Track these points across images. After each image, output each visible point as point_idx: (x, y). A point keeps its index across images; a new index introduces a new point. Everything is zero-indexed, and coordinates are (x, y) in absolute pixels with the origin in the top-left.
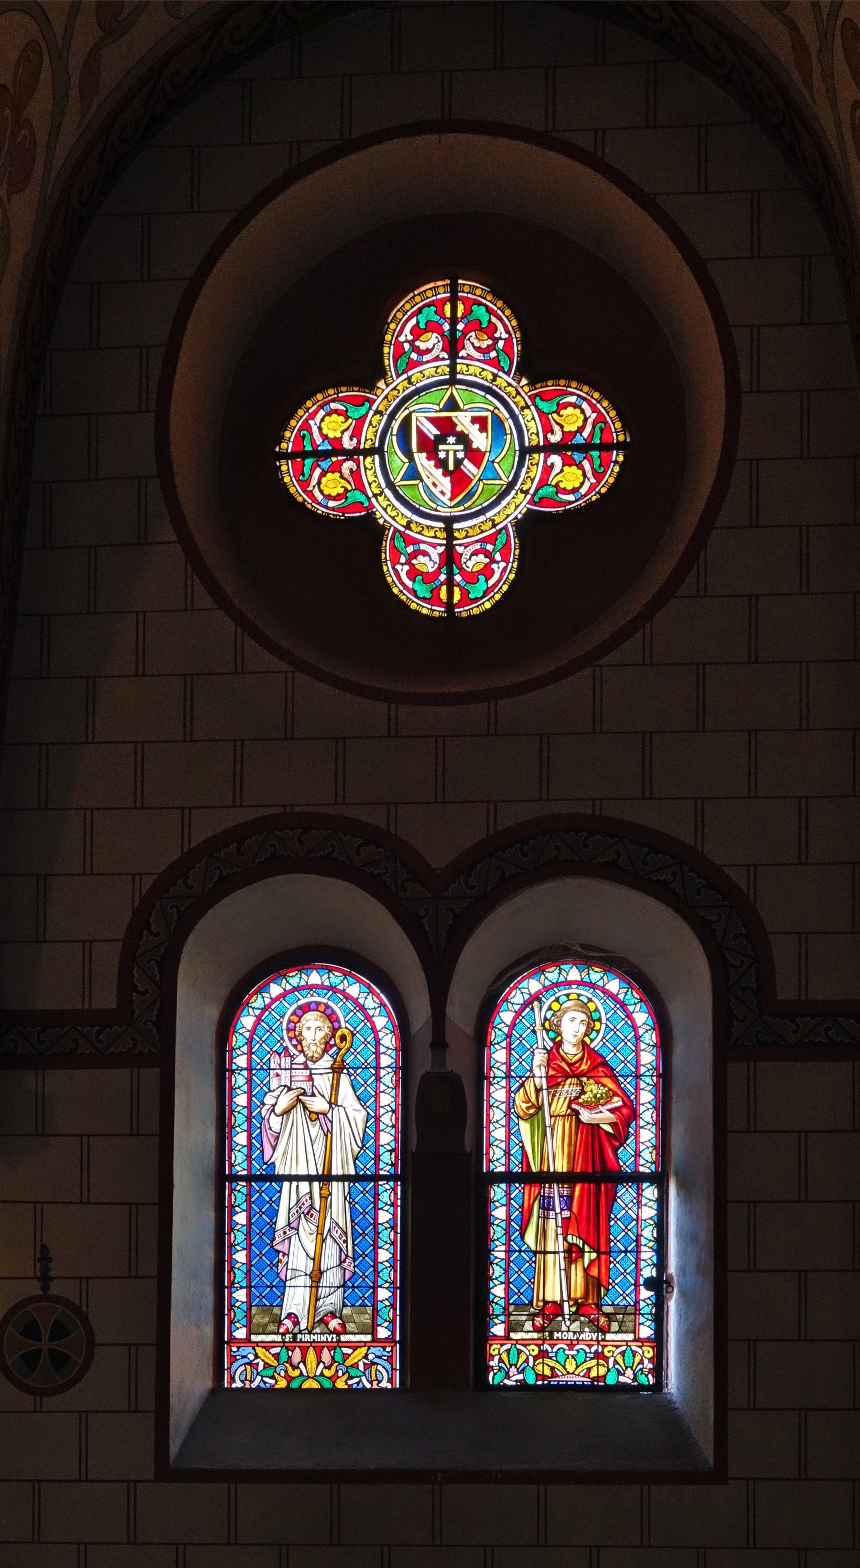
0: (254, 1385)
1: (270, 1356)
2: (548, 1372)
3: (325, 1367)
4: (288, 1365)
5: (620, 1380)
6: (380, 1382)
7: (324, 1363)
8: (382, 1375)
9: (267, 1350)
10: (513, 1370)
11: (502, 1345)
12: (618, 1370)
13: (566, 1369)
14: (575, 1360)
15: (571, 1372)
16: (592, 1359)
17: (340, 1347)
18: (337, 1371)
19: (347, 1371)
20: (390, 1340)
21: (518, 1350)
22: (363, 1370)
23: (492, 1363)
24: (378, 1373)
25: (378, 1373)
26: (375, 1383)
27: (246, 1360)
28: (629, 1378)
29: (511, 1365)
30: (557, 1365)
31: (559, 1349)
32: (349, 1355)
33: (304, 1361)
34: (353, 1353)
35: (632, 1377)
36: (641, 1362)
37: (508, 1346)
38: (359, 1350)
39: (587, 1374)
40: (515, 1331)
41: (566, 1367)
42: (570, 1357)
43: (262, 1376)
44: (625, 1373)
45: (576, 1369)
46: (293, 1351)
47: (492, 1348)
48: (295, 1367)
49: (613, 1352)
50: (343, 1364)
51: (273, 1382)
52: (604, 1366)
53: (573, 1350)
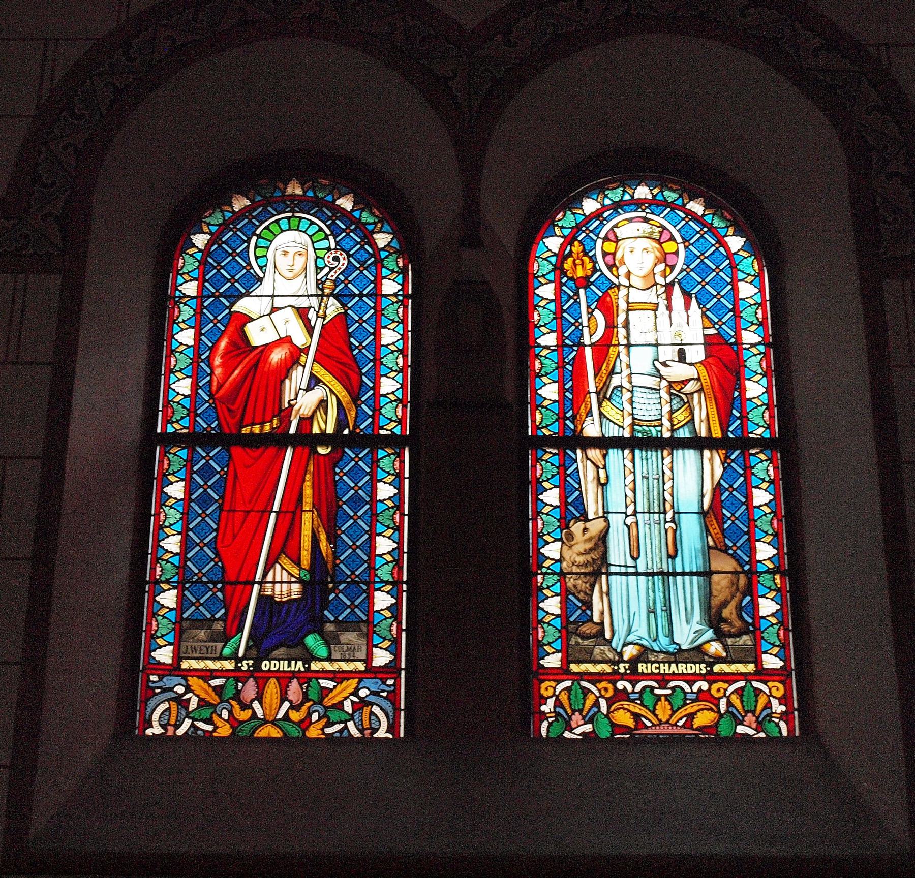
0: (180, 732)
1: (210, 690)
2: (630, 723)
3: (292, 707)
4: (234, 703)
5: (738, 731)
6: (376, 730)
7: (291, 702)
8: (379, 721)
9: (206, 681)
10: (577, 717)
11: (559, 682)
12: (734, 716)
13: (656, 716)
14: (670, 704)
15: (664, 720)
16: (693, 701)
17: (317, 679)
18: (309, 715)
19: (325, 716)
20: (391, 669)
21: (583, 688)
22: (350, 712)
23: (543, 708)
24: (373, 717)
25: (373, 717)
26: (367, 732)
27: (171, 695)
28: (749, 727)
29: (574, 711)
30: (644, 712)
31: (644, 688)
32: (331, 690)
33: (260, 698)
35: (754, 725)
36: (768, 705)
37: (568, 683)
38: (345, 684)
39: (689, 724)
40: (579, 662)
41: (657, 712)
42: (663, 698)
43: (194, 719)
44: (744, 720)
45: (671, 716)
47: (544, 686)
48: (245, 706)
49: (726, 690)
50: (320, 702)
51: (209, 728)
52: (711, 709)
53: (665, 688)
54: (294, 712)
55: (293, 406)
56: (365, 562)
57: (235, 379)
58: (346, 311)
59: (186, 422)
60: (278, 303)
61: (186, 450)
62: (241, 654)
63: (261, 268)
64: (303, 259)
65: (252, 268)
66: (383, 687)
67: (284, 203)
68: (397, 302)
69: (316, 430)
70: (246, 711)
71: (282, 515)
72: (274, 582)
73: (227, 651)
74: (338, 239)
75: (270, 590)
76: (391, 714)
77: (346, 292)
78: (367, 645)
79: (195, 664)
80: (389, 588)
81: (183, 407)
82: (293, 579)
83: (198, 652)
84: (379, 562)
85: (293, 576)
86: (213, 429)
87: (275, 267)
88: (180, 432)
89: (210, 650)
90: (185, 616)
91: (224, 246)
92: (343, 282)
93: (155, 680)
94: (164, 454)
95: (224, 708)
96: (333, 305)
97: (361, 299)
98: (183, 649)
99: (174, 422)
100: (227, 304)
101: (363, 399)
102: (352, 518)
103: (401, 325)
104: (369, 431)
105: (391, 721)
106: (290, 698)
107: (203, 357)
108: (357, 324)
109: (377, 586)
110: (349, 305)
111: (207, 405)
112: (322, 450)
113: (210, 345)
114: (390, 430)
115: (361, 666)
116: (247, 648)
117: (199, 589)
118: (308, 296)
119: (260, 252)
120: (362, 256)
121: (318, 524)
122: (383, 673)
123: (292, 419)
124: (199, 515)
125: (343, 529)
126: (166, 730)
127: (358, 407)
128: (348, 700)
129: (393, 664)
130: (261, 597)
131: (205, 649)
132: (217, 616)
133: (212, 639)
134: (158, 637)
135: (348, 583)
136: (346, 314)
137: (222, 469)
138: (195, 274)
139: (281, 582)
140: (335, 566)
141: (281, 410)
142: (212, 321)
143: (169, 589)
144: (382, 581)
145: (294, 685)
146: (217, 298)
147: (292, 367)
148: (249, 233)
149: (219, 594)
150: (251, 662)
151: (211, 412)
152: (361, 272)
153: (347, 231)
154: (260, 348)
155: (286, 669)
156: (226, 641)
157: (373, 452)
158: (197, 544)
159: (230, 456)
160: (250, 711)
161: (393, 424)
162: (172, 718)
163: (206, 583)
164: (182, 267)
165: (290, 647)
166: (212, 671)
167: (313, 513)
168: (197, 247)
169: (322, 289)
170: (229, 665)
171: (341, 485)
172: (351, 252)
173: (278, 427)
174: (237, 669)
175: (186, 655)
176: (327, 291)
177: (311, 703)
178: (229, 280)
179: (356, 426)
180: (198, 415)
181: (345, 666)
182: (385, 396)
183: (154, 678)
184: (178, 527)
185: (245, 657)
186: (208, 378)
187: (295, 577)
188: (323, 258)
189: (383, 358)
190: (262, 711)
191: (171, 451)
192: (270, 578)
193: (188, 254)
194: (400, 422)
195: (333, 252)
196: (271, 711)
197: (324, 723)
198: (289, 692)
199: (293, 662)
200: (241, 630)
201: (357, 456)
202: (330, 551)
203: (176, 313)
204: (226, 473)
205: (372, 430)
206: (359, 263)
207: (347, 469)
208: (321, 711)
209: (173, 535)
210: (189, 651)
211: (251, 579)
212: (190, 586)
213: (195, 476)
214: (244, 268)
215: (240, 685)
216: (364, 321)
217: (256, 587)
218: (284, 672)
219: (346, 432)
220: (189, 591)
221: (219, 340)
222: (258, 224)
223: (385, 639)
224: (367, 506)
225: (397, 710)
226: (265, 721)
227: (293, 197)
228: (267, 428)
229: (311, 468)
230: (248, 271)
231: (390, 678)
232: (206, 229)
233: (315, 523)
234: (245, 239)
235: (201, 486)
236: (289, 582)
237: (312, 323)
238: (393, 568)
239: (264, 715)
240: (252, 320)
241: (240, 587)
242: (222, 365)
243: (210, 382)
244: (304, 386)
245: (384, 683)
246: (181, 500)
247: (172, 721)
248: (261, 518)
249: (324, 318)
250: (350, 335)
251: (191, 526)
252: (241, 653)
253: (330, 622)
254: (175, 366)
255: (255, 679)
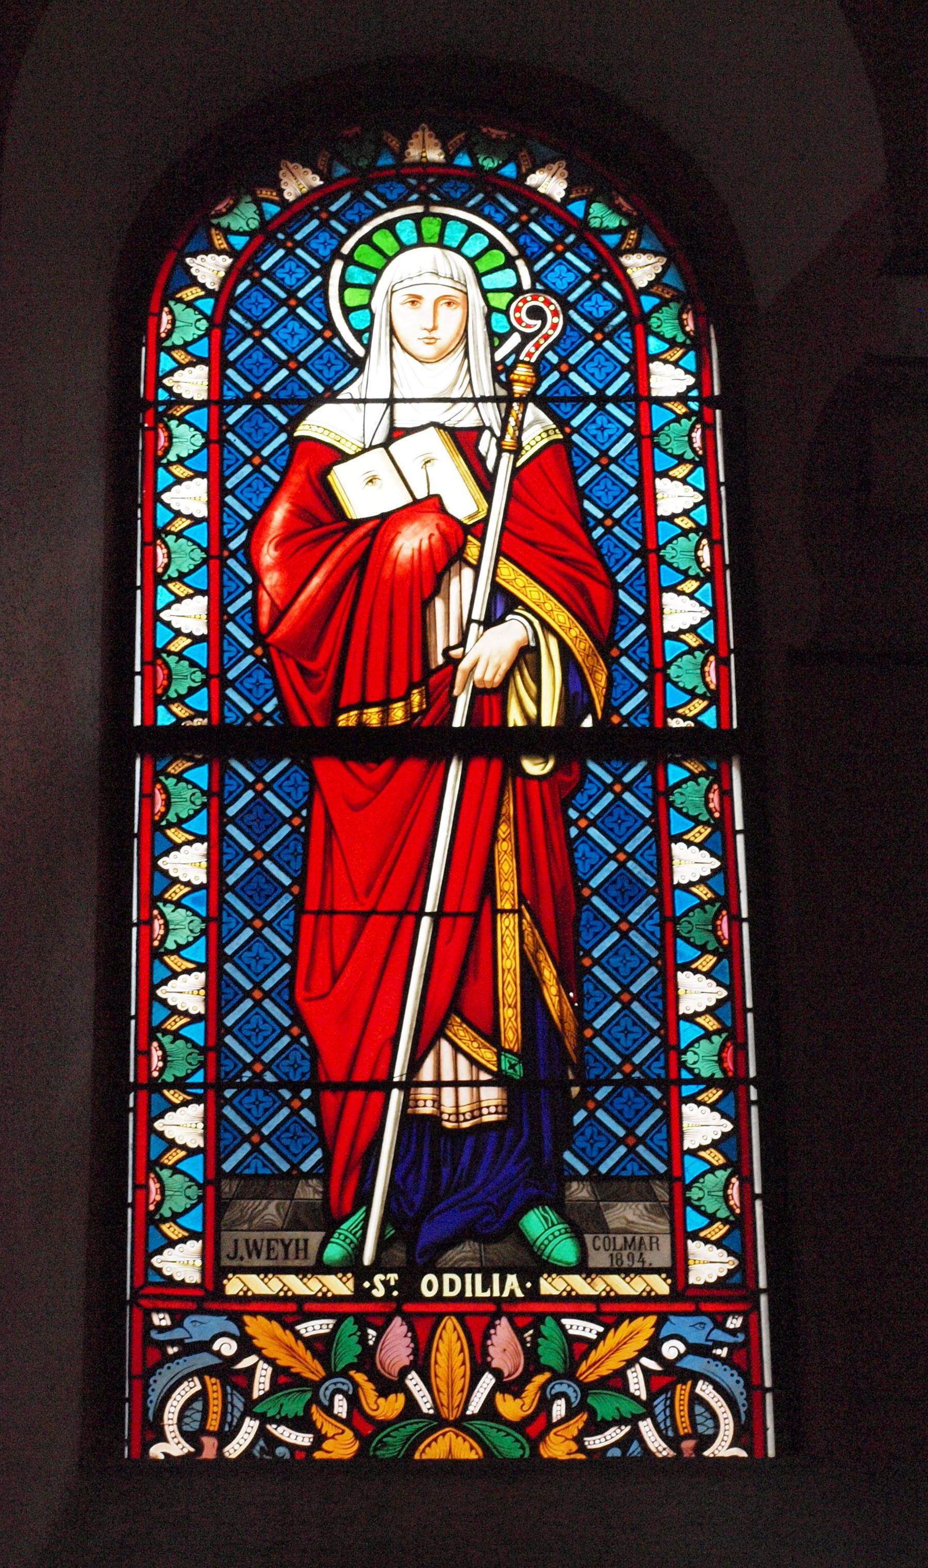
0: (234, 1450)
1: (300, 1348)
3: (502, 1386)
4: (360, 1378)
6: (709, 1440)
7: (497, 1373)
9: (289, 1326)
17: (557, 1317)
18: (545, 1404)
19: (584, 1406)
22: (644, 1397)
24: (699, 1409)
25: (699, 1409)
32: (593, 1344)
34: (602, 1336)
38: (625, 1328)
43: (264, 1419)
46: (381, 1332)
50: (570, 1374)
51: (304, 1439)
54: (509, 1397)
55: (459, 661)
56: (654, 1033)
57: (313, 599)
58: (568, 437)
59: (200, 701)
60: (405, 416)
61: (204, 769)
62: (368, 1257)
63: (358, 334)
64: (457, 313)
65: (336, 334)
66: (718, 1335)
67: (402, 179)
68: (687, 416)
69: (515, 718)
70: (392, 1397)
71: (445, 922)
72: (438, 1084)
73: (333, 1252)
74: (538, 267)
75: (429, 1103)
76: (741, 1400)
77: (565, 391)
78: (673, 1232)
79: (257, 1285)
80: (713, 1095)
81: (193, 664)
82: (484, 1077)
83: (264, 1255)
84: (688, 1033)
85: (481, 1067)
86: (268, 717)
87: (392, 332)
88: (189, 723)
89: (292, 1248)
90: (227, 1167)
91: (266, 281)
92: (554, 367)
93: (163, 1323)
94: (154, 777)
95: (338, 1391)
96: (536, 421)
97: (601, 408)
98: (227, 1247)
99: (173, 701)
100: (283, 420)
101: (623, 645)
102: (615, 927)
103: (700, 471)
104: (642, 721)
105: (743, 1417)
106: (494, 1364)
107: (233, 545)
108: (596, 469)
109: (687, 1090)
110: (575, 423)
111: (249, 659)
112: (533, 767)
113: (248, 516)
114: (694, 719)
115: (661, 1286)
116: (382, 1244)
117: (257, 1102)
118: (475, 401)
119: (354, 297)
120: (597, 306)
121: (536, 943)
122: (720, 1299)
123: (455, 692)
124: (248, 923)
125: (596, 954)
126: (199, 1448)
127: (611, 663)
128: (638, 1367)
129: (737, 1279)
130: (408, 1120)
131: (280, 1248)
132: (306, 1167)
133: (295, 1224)
134: (164, 1220)
135: (617, 1083)
136: (567, 442)
137: (296, 813)
138: (201, 349)
139: (456, 1084)
140: (583, 1043)
141: (428, 672)
142: (248, 460)
143: (185, 1104)
144: (697, 1079)
145: (503, 1332)
146: (258, 405)
147: (447, 568)
148: (324, 252)
149: (307, 1115)
150: (393, 1277)
151: (260, 675)
152: (598, 345)
153: (558, 248)
154: (370, 525)
155: (479, 1293)
156: (330, 1226)
157: (656, 770)
158: (248, 994)
159: (313, 781)
160: (401, 1397)
161: (699, 705)
162: (212, 1416)
163: (273, 1088)
164: (170, 333)
165: (485, 1239)
166: (300, 1300)
167: (521, 917)
168: (203, 286)
169: (508, 386)
170: (340, 1286)
171: (582, 849)
172: (572, 297)
173: (421, 712)
174: (362, 1295)
175: (235, 1263)
176: (518, 389)
177: (547, 1375)
178: (282, 364)
179: (611, 708)
180: (231, 684)
181: (621, 1285)
182: (675, 636)
183: (161, 1319)
184: (198, 952)
185: (379, 1266)
186: (248, 596)
187: (488, 1071)
188: (506, 313)
189: (664, 546)
190: (428, 1397)
191: (170, 770)
192: (427, 1073)
193: (180, 300)
194: (714, 698)
195: (528, 297)
196: (451, 1396)
197: (581, 1425)
198: (491, 1350)
199: (496, 1277)
200: (367, 1200)
201: (618, 779)
202: (567, 1006)
203: (162, 442)
204: (306, 821)
205: (651, 719)
206: (591, 323)
207: (596, 810)
208: (572, 1395)
209: (188, 972)
210: (242, 1251)
211: (381, 1076)
212: (234, 1096)
213: (231, 829)
214: (318, 334)
215: (372, 1333)
216: (614, 460)
217: (396, 1096)
218: (474, 1299)
219: (588, 723)
220: (234, 1108)
221: (269, 504)
222: (343, 230)
223: (713, 1219)
224: (651, 900)
225: (754, 1388)
226: (437, 1422)
227: (426, 166)
228: (398, 714)
229: (509, 808)
230: (328, 342)
231: (735, 1313)
232: (219, 241)
233: (529, 939)
234: (316, 265)
235: (248, 854)
236: (475, 1084)
237: (490, 465)
238: (723, 1046)
239: (435, 1407)
240: (343, 457)
241: (356, 1097)
242: (281, 564)
243: (254, 605)
244: (479, 613)
245: (720, 1325)
246: (201, 887)
247: (213, 1424)
248: (397, 928)
249: (517, 450)
250: (581, 494)
251: (229, 950)
252: (368, 1257)
253: (577, 1177)
254: (167, 567)
255: (408, 1319)
